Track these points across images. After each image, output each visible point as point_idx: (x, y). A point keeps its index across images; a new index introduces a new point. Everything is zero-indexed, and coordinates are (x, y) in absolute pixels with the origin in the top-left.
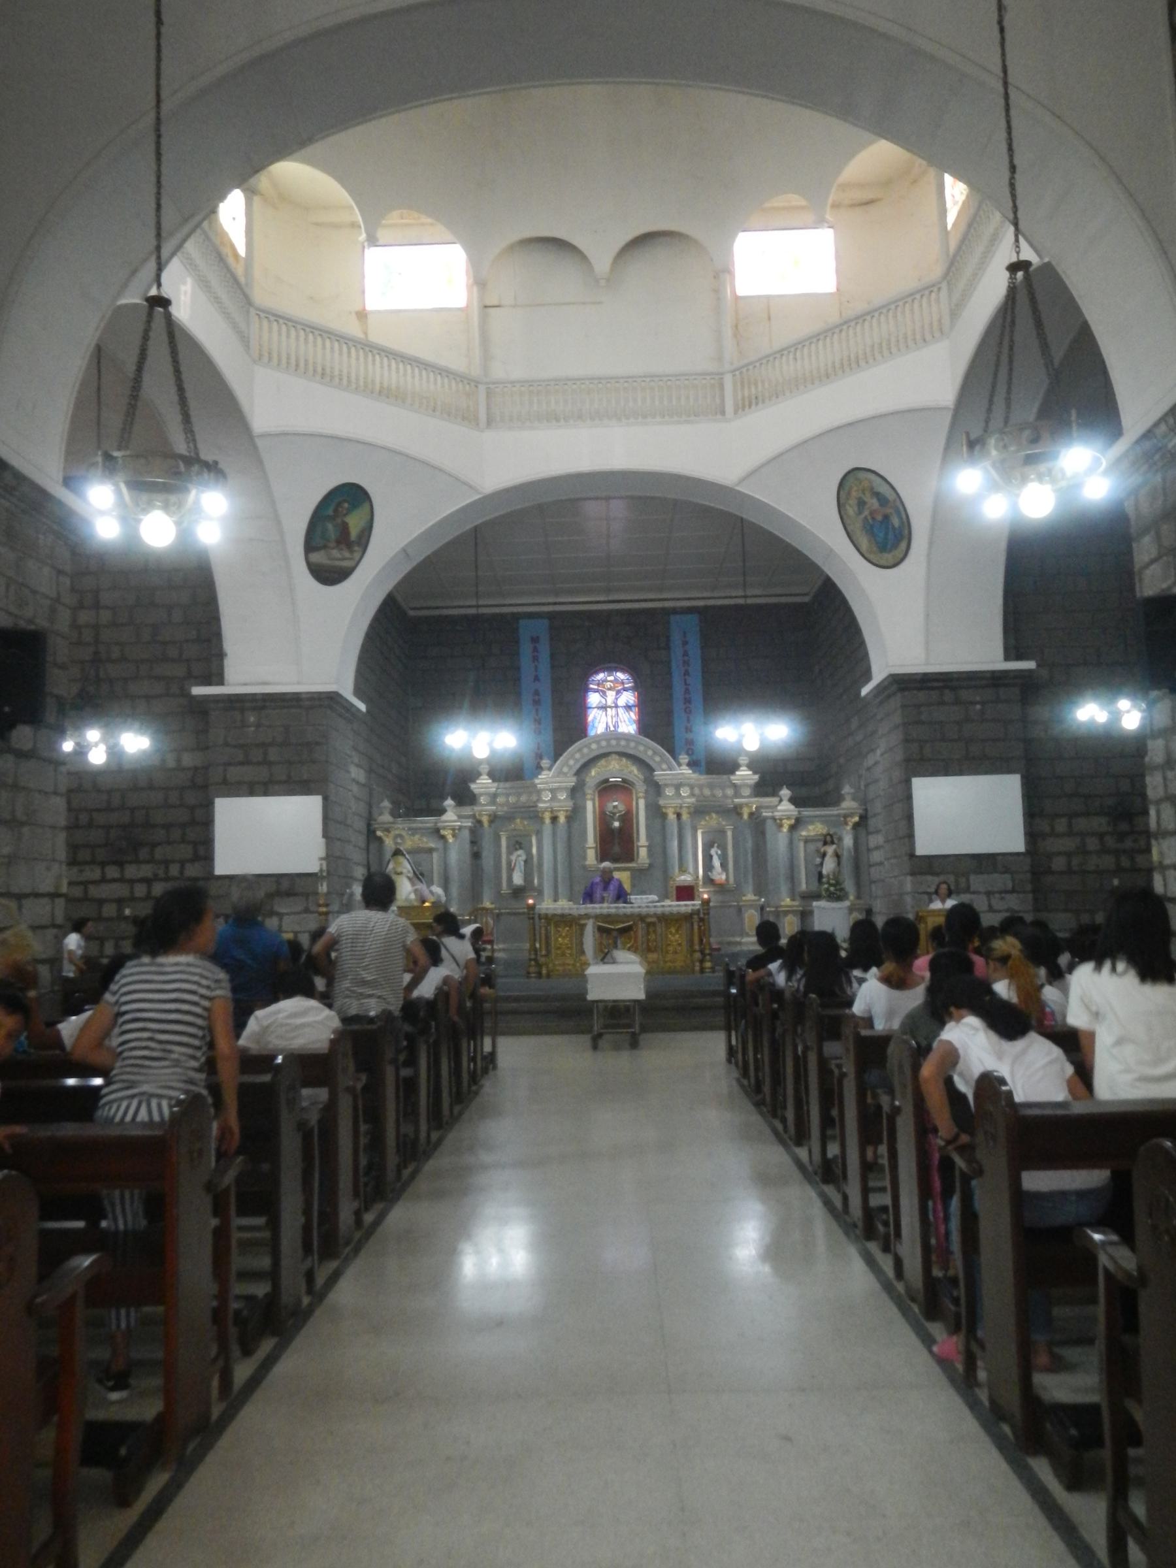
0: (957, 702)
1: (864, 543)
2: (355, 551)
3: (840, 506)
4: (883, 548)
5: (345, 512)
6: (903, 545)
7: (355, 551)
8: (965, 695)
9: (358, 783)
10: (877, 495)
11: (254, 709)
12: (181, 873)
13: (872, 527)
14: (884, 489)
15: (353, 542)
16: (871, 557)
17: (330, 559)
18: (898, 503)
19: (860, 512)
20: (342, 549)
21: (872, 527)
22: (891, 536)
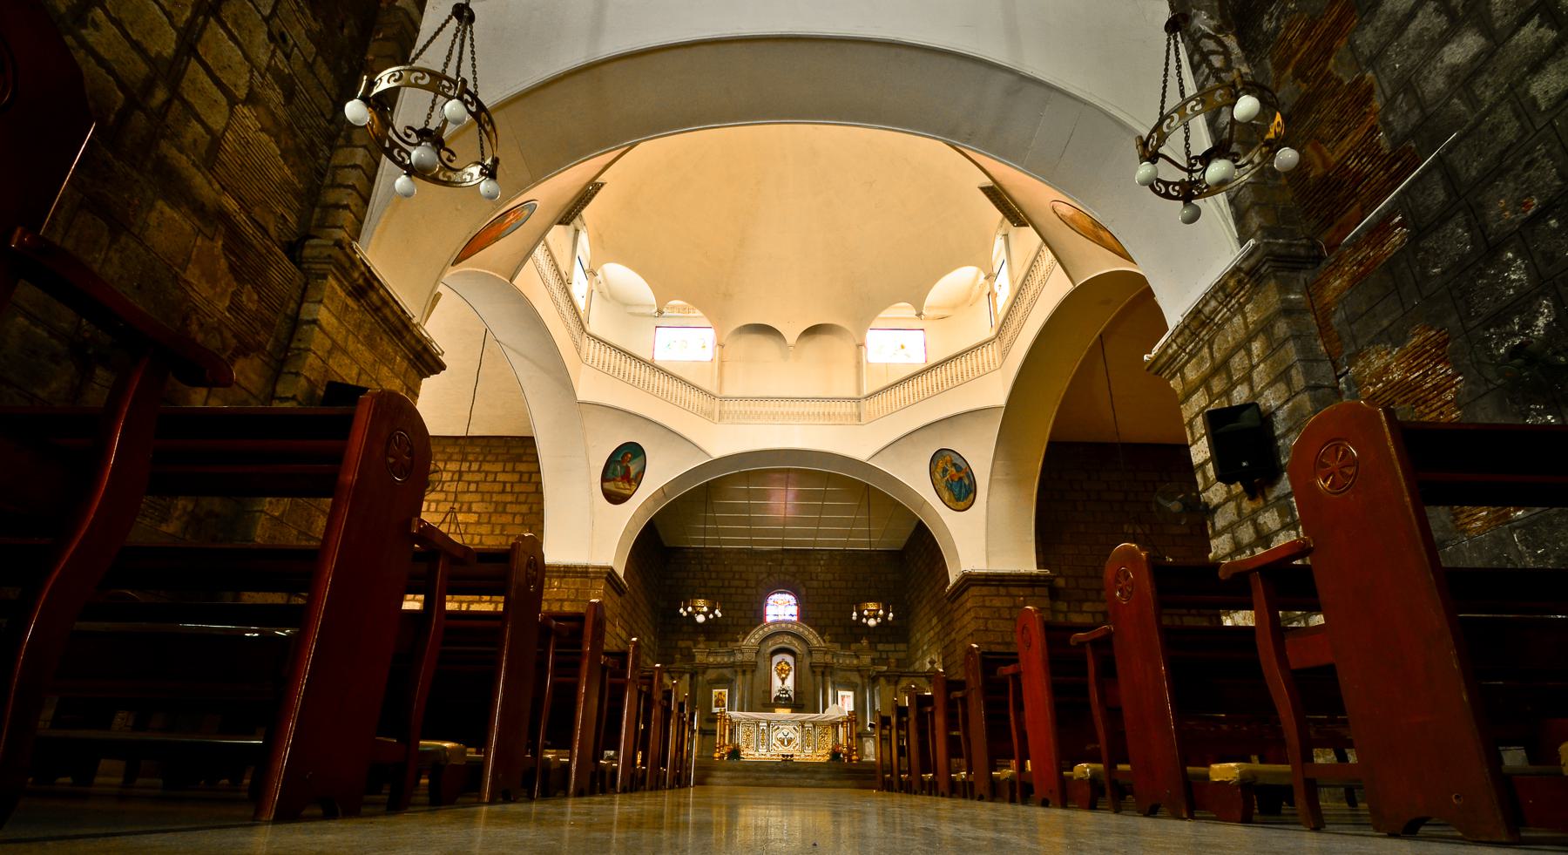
0: (1009, 595)
1: (946, 496)
3: (931, 474)
4: (958, 500)
6: (972, 496)
8: (1014, 591)
10: (954, 465)
11: (558, 577)
13: (951, 485)
14: (959, 462)
16: (951, 504)
18: (968, 470)
19: (944, 477)
21: (951, 485)
22: (963, 490)
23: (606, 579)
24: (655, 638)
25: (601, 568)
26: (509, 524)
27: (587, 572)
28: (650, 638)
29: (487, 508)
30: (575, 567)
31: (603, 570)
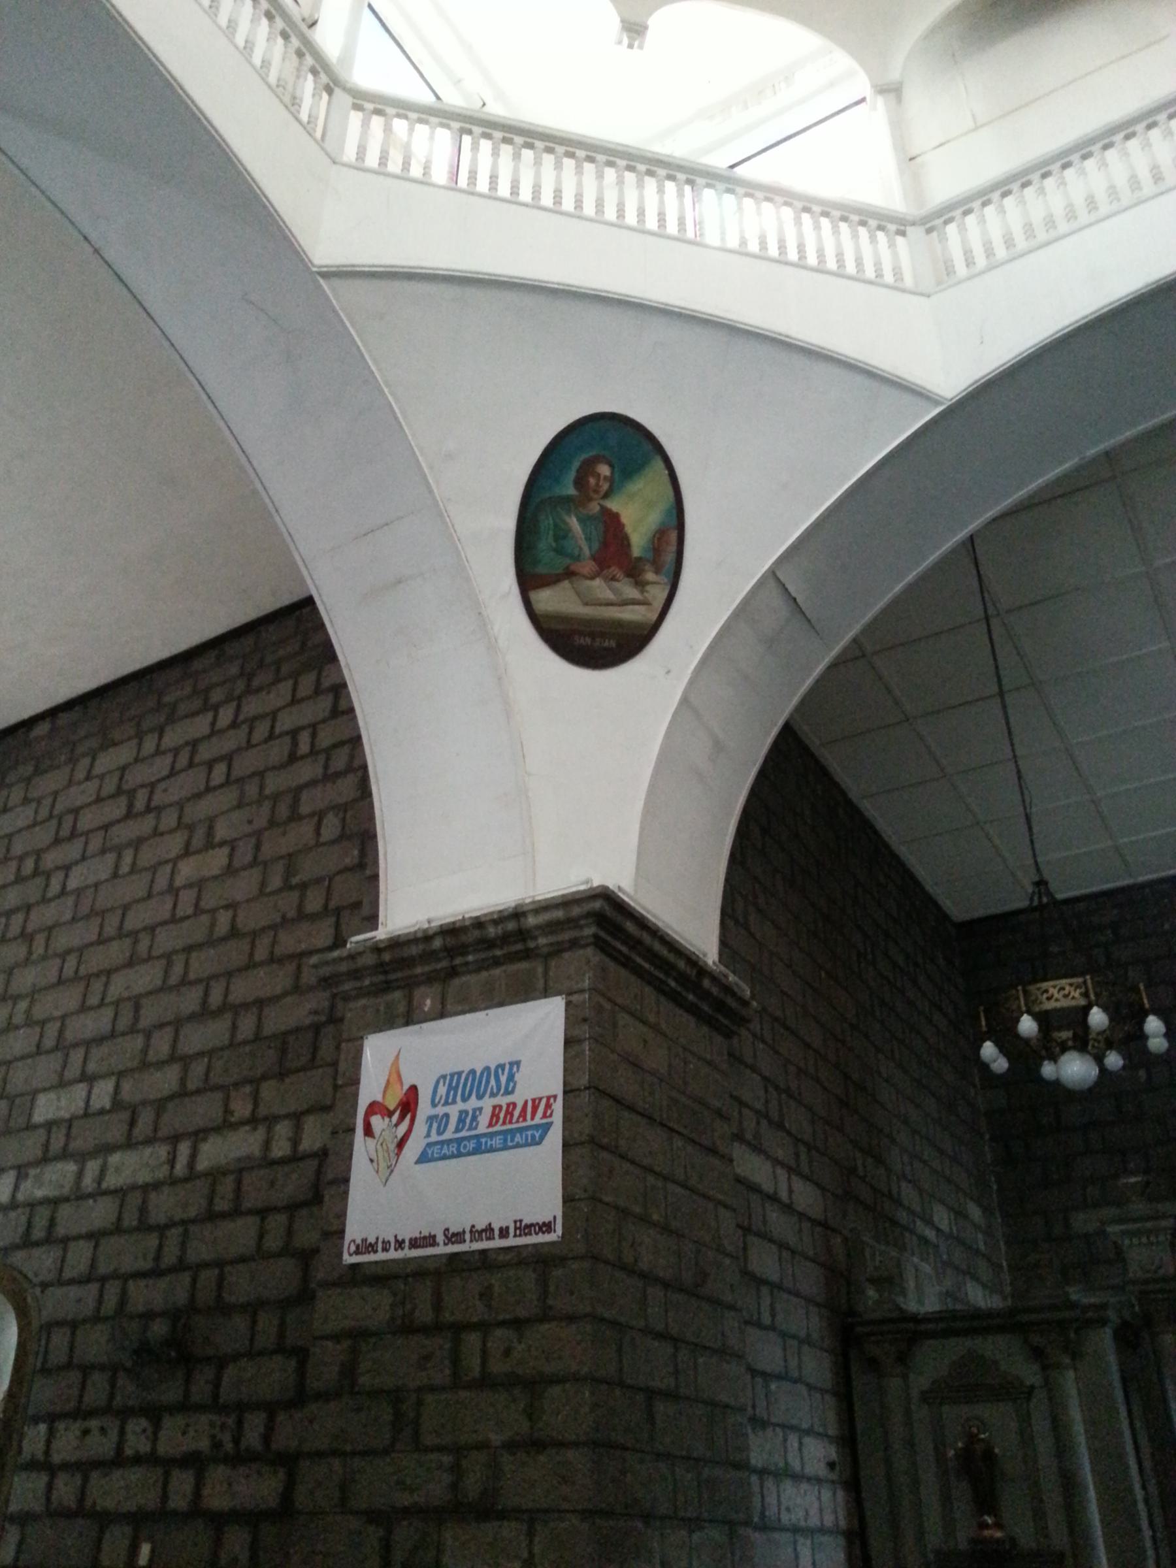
2: (648, 583)
5: (605, 486)
7: (648, 583)
9: (788, 1208)
11: (429, 979)
12: (266, 1439)
15: (639, 559)
17: (586, 604)
20: (613, 579)
23: (599, 944)
24: (987, 1210)
25: (567, 902)
26: (307, 849)
27: (523, 935)
28: (960, 1214)
29: (250, 822)
30: (478, 923)
31: (576, 911)
